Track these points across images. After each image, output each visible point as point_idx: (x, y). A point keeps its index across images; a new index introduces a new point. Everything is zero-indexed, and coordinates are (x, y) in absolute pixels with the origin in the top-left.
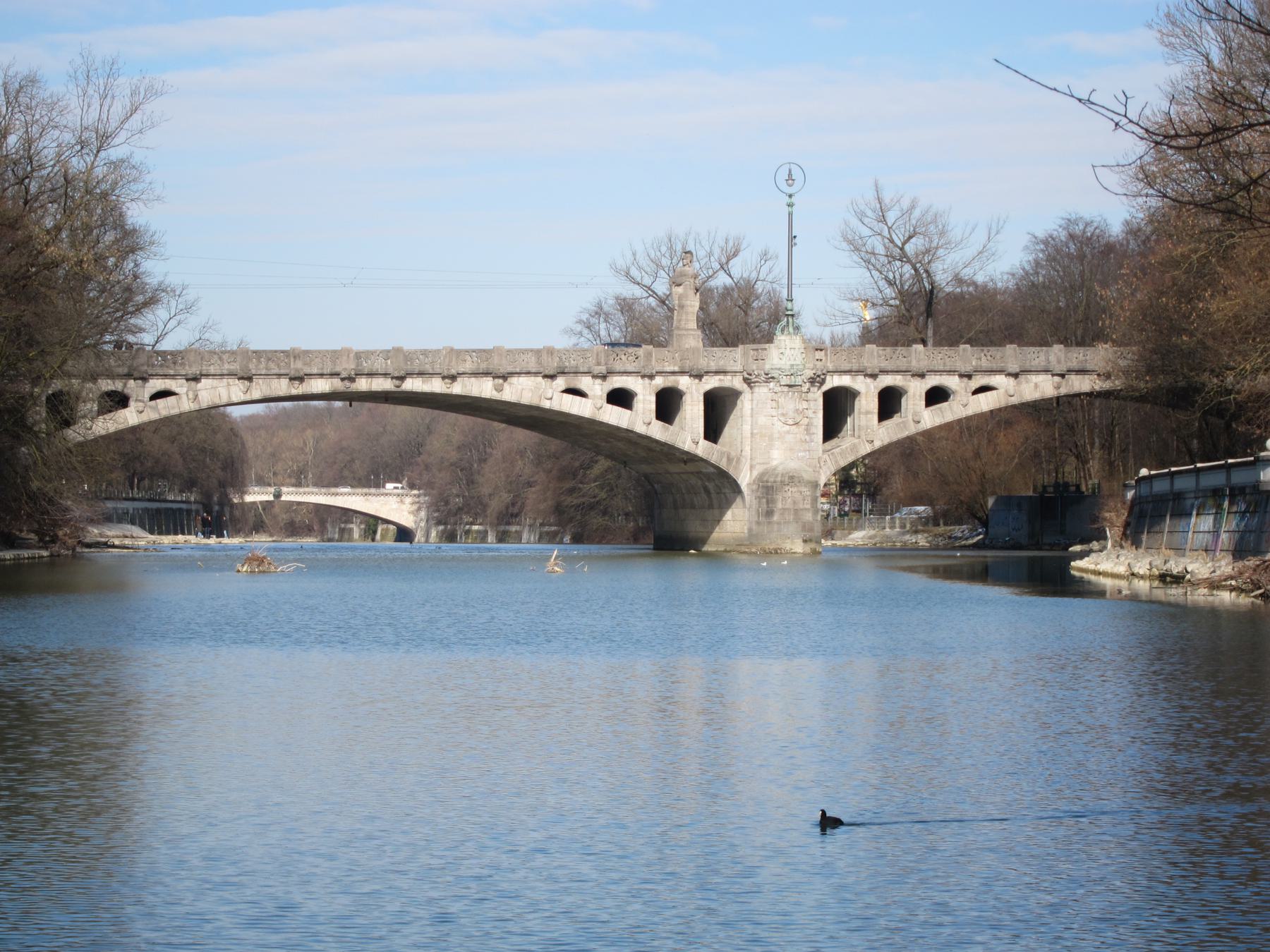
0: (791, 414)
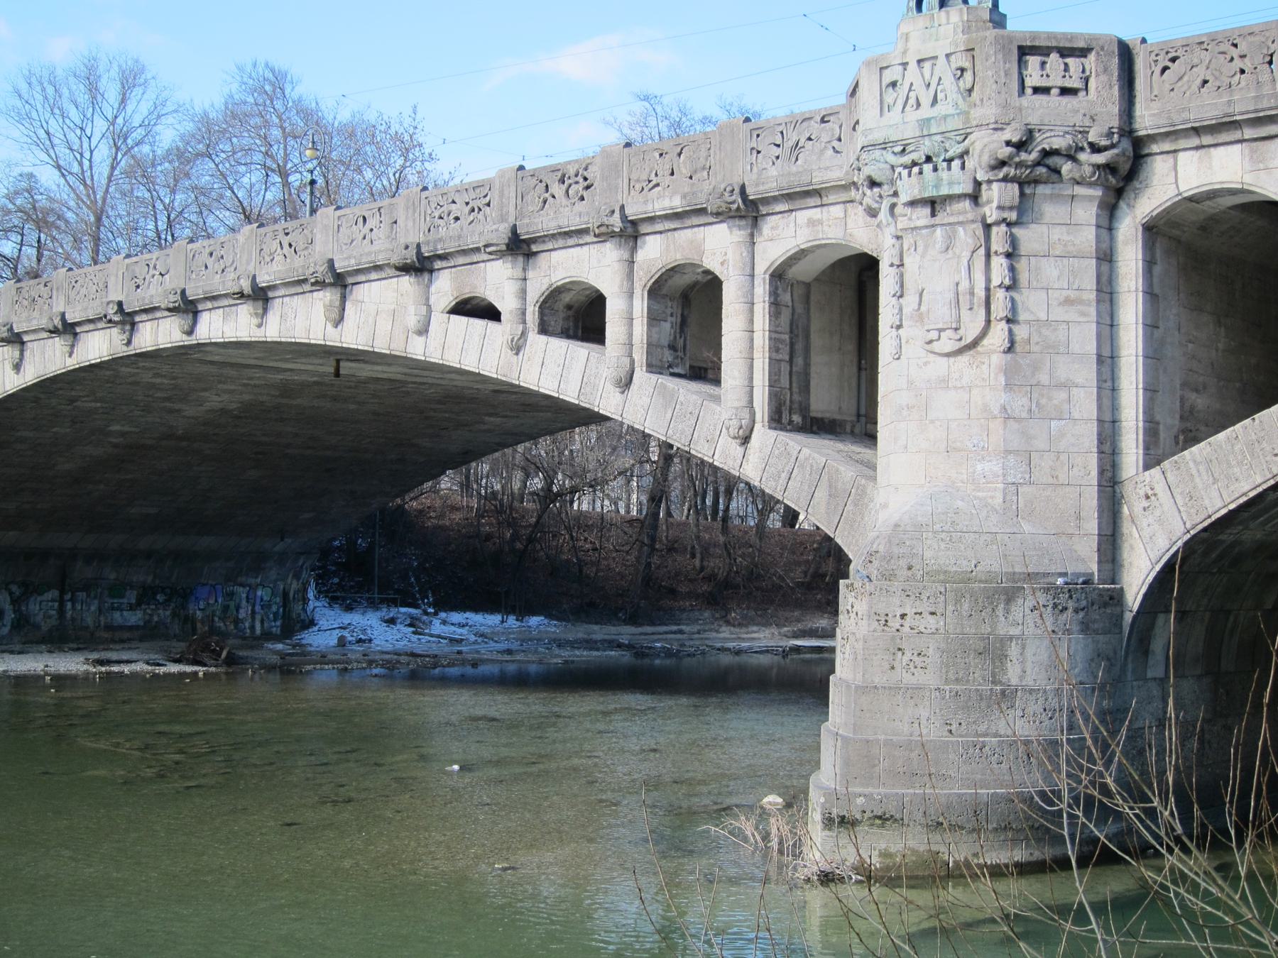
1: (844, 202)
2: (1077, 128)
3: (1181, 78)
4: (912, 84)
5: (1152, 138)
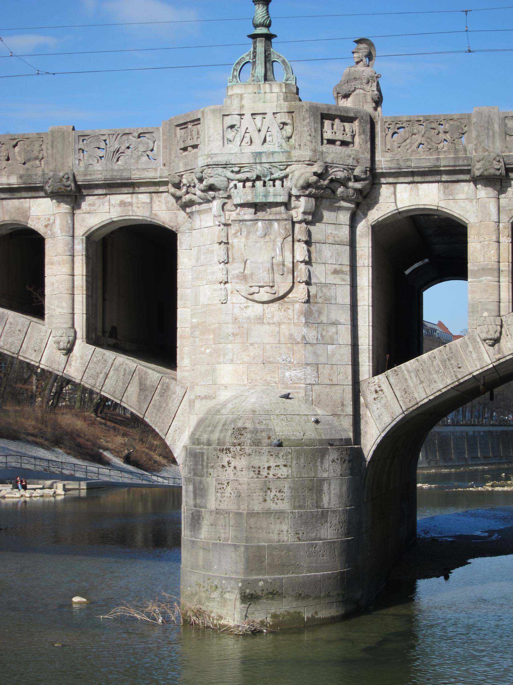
0: (264, 277)
1: (150, 193)
2: (350, 167)
3: (405, 141)
4: (247, 128)
5: (384, 175)
